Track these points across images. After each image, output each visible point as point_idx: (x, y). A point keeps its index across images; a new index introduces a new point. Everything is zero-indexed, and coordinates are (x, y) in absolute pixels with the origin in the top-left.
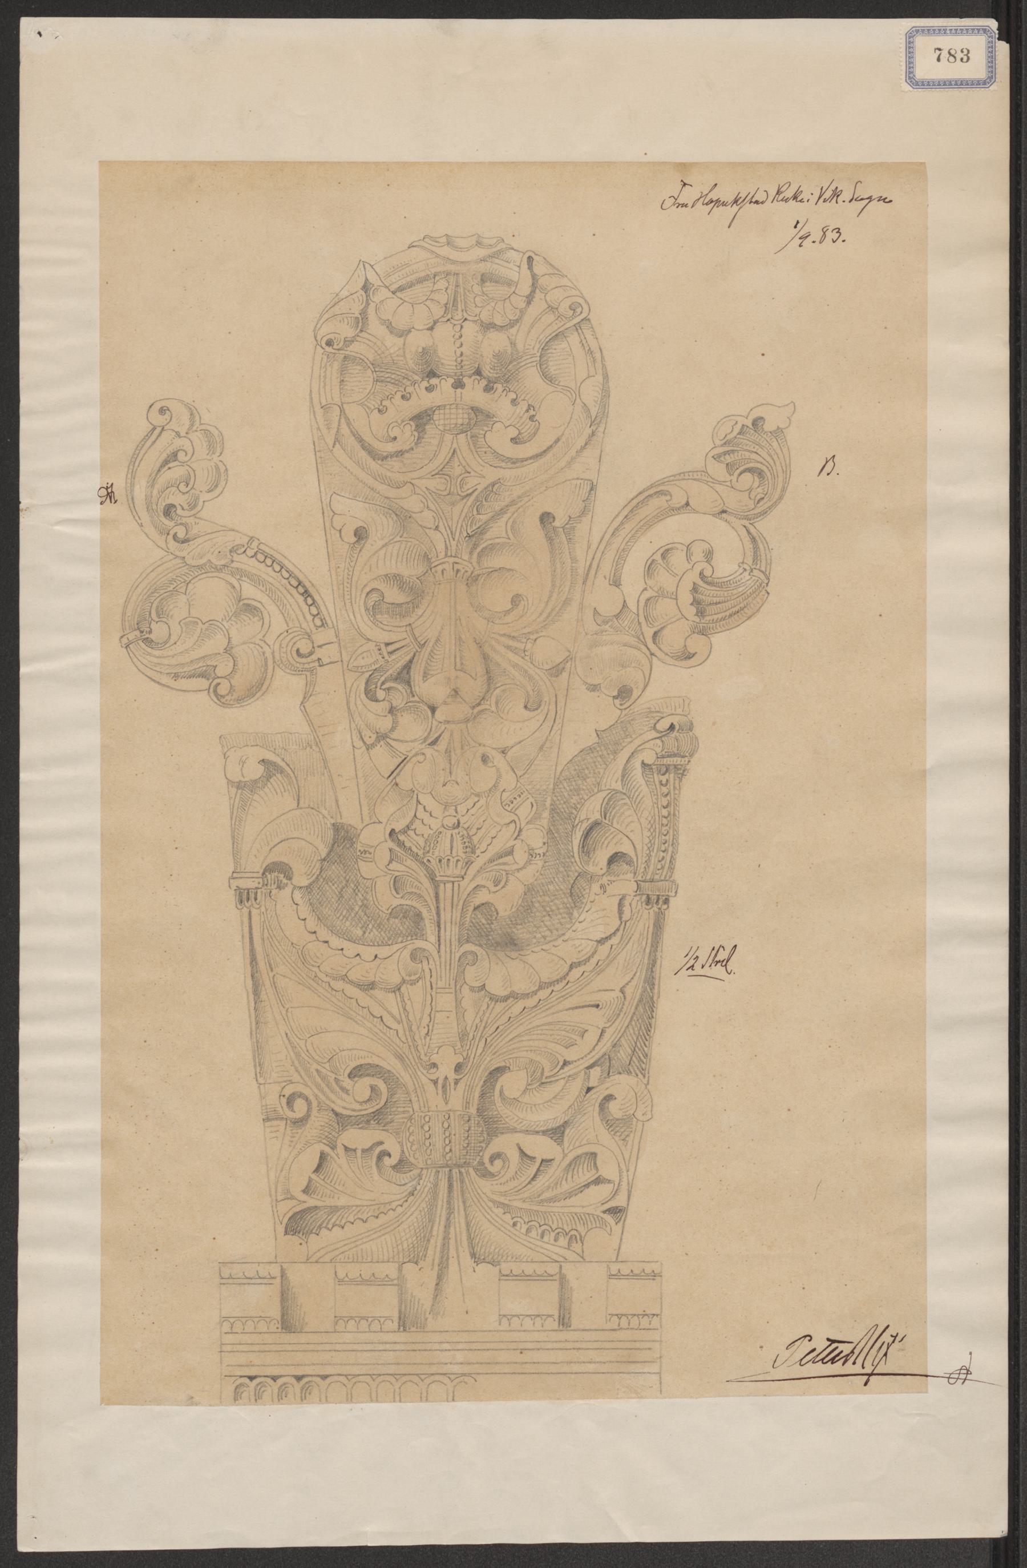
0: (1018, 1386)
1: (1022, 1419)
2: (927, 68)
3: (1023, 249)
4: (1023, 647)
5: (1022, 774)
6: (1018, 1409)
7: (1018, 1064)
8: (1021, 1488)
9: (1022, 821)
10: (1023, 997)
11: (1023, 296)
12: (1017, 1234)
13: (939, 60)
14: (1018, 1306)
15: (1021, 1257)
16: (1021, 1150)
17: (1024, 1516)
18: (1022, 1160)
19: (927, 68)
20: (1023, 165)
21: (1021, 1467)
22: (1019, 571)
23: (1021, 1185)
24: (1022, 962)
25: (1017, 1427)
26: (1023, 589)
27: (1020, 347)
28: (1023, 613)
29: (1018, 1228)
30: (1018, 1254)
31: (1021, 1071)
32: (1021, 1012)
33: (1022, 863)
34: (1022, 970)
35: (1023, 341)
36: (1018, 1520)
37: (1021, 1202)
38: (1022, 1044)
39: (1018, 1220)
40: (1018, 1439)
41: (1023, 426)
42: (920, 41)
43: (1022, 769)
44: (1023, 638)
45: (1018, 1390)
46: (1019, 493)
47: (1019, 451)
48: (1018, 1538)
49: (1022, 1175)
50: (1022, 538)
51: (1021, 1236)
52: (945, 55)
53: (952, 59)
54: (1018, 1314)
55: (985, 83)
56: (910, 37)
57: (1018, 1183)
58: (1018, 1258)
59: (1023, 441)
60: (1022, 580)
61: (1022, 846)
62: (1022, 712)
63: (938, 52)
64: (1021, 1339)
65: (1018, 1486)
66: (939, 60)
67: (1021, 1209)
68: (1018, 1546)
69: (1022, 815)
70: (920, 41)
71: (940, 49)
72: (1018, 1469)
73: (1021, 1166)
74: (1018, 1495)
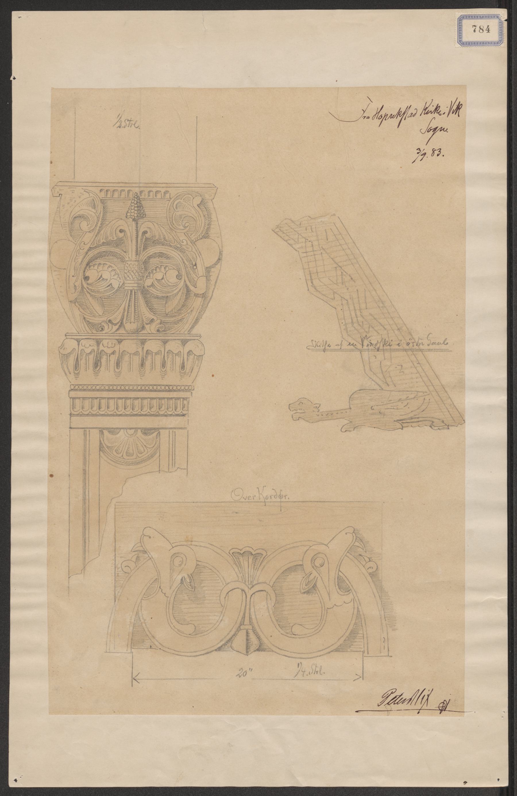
0: (513, 663)
1: (515, 679)
2: (468, 35)
3: (513, 87)
4: (514, 288)
5: (514, 353)
7: (512, 500)
8: (515, 714)
9: (514, 376)
10: (514, 466)
11: (513, 111)
12: (512, 585)
13: (475, 31)
14: (513, 622)
15: (514, 597)
16: (514, 543)
17: (516, 729)
18: (514, 549)
19: (468, 35)
20: (513, 45)
23: (514, 561)
24: (514, 448)
25: (513, 683)
26: (513, 259)
27: (512, 137)
28: (514, 271)
30: (513, 595)
32: (514, 473)
33: (514, 398)
35: (513, 134)
36: (513, 731)
37: (514, 569)
38: (514, 490)
39: (512, 579)
40: (513, 690)
42: (465, 22)
43: (514, 350)
44: (514, 284)
46: (512, 211)
47: (512, 189)
48: (513, 739)
49: (514, 556)
50: (514, 234)
51: (514, 587)
52: (478, 29)
53: (481, 31)
54: (513, 626)
55: (498, 43)
56: (461, 19)
59: (513, 184)
60: (513, 255)
61: (514, 389)
62: (514, 321)
63: (474, 27)
64: (515, 639)
65: (513, 713)
66: (475, 31)
67: (514, 573)
68: (513, 744)
69: (514, 374)
70: (465, 22)
71: (475, 26)
72: (513, 704)
73: (514, 551)
74: (513, 718)
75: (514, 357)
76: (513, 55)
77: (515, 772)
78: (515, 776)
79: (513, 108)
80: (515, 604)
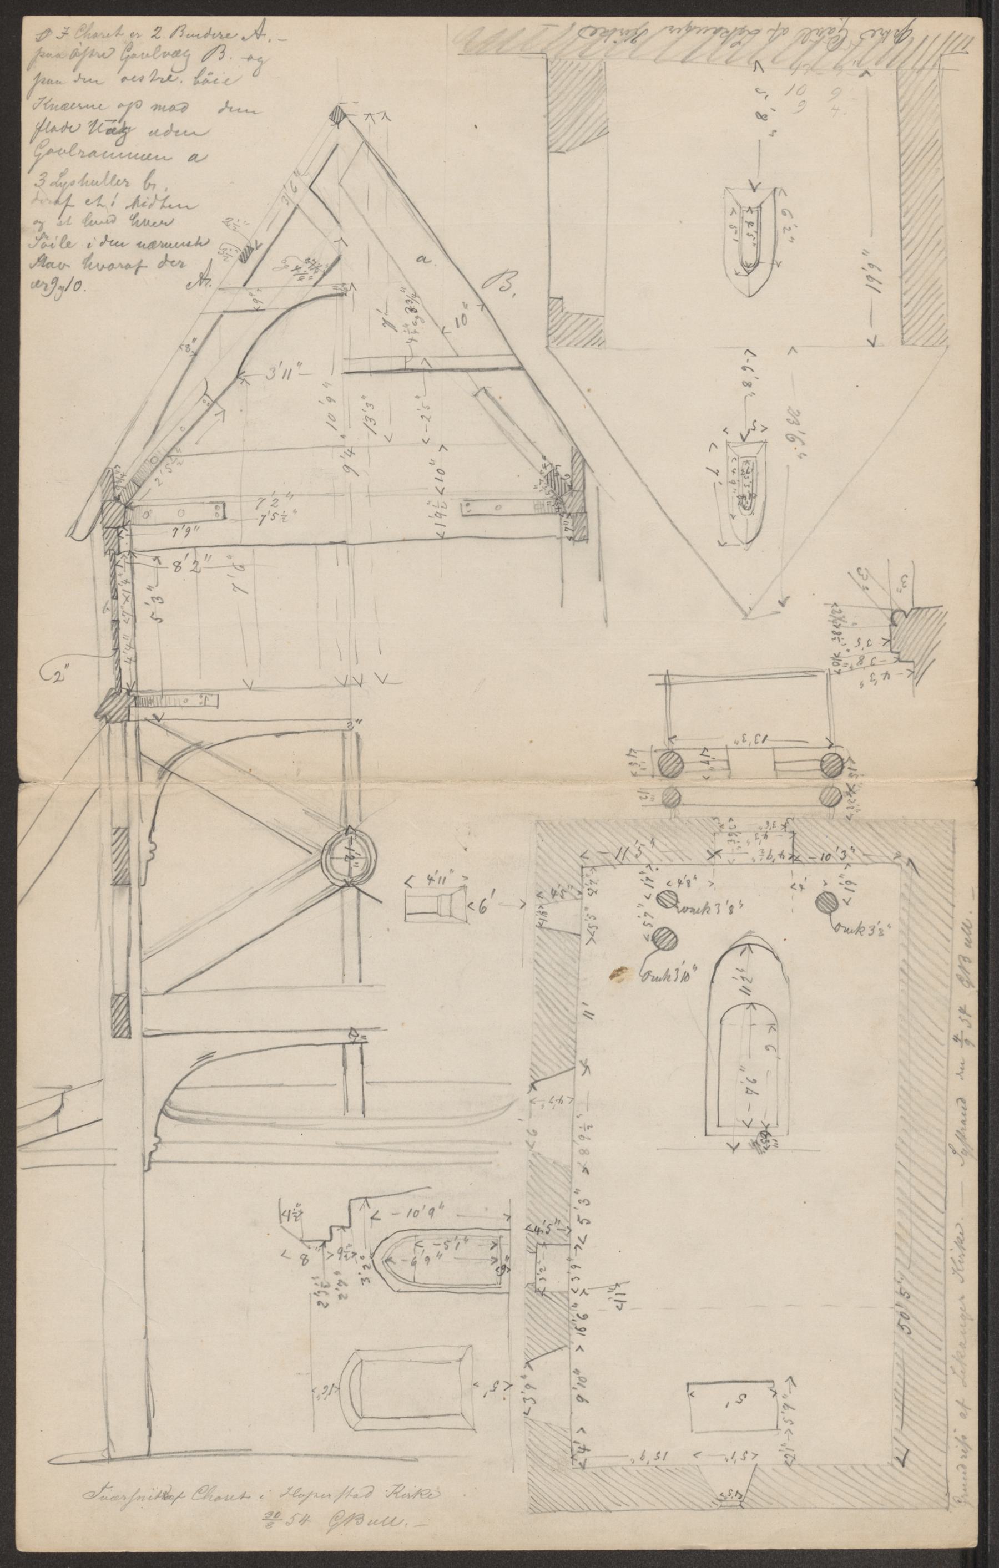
1: (991, 1171)
6: (987, 1162)
7: (987, 850)
9: (991, 629)
11: (993, 155)
15: (990, 1025)
18: (991, 937)
21: (990, 1216)
22: (989, 403)
26: (992, 419)
28: (992, 441)
29: (987, 999)
31: (991, 857)
33: (991, 667)
34: (991, 765)
35: (993, 194)
37: (990, 974)
39: (987, 991)
41: (992, 272)
44: (992, 463)
45: (987, 1147)
48: (987, 1280)
50: (992, 374)
57: (987, 958)
58: (987, 1026)
59: (993, 285)
61: (992, 652)
64: (990, 1099)
68: (987, 1287)
69: (991, 624)
72: (987, 1217)
73: (990, 942)
74: (987, 1240)
75: (992, 596)
76: (993, 54)
77: (990, 1337)
78: (990, 1345)
79: (992, 151)
80: (991, 1037)
